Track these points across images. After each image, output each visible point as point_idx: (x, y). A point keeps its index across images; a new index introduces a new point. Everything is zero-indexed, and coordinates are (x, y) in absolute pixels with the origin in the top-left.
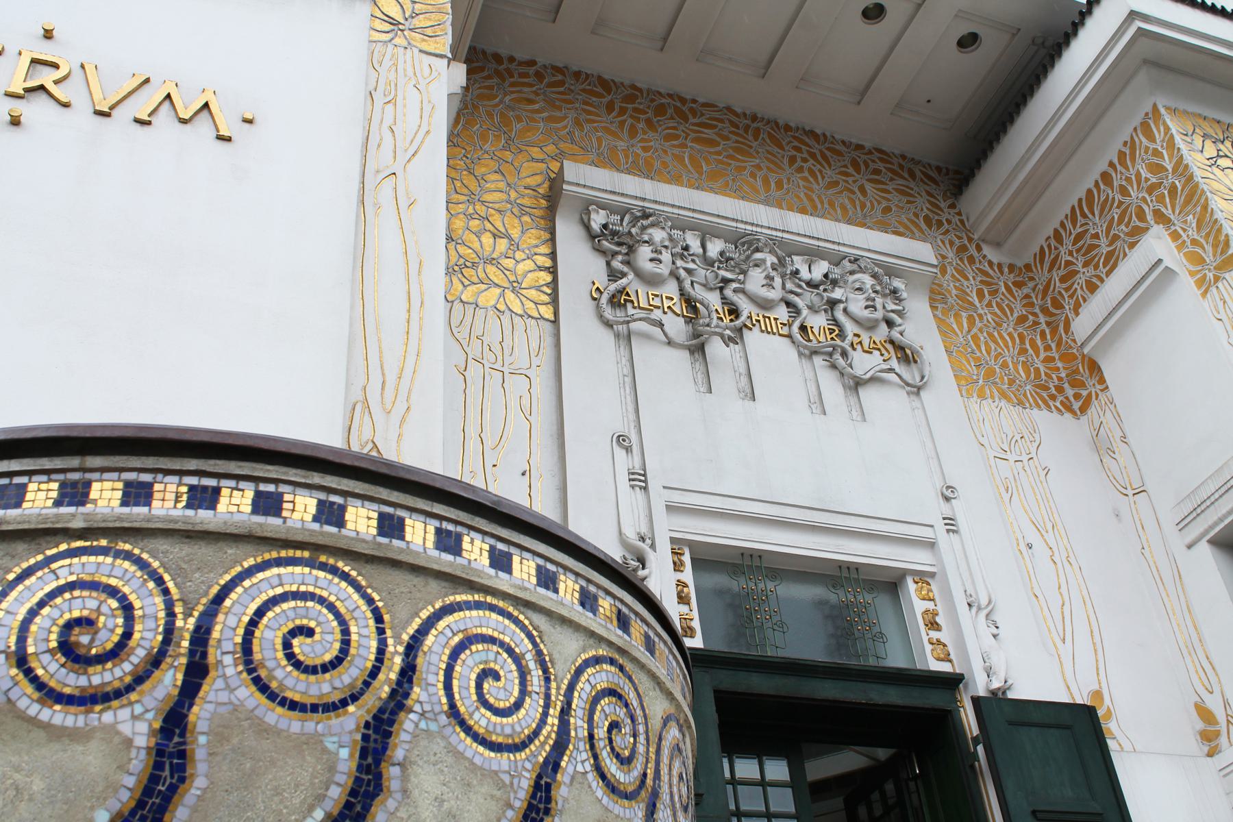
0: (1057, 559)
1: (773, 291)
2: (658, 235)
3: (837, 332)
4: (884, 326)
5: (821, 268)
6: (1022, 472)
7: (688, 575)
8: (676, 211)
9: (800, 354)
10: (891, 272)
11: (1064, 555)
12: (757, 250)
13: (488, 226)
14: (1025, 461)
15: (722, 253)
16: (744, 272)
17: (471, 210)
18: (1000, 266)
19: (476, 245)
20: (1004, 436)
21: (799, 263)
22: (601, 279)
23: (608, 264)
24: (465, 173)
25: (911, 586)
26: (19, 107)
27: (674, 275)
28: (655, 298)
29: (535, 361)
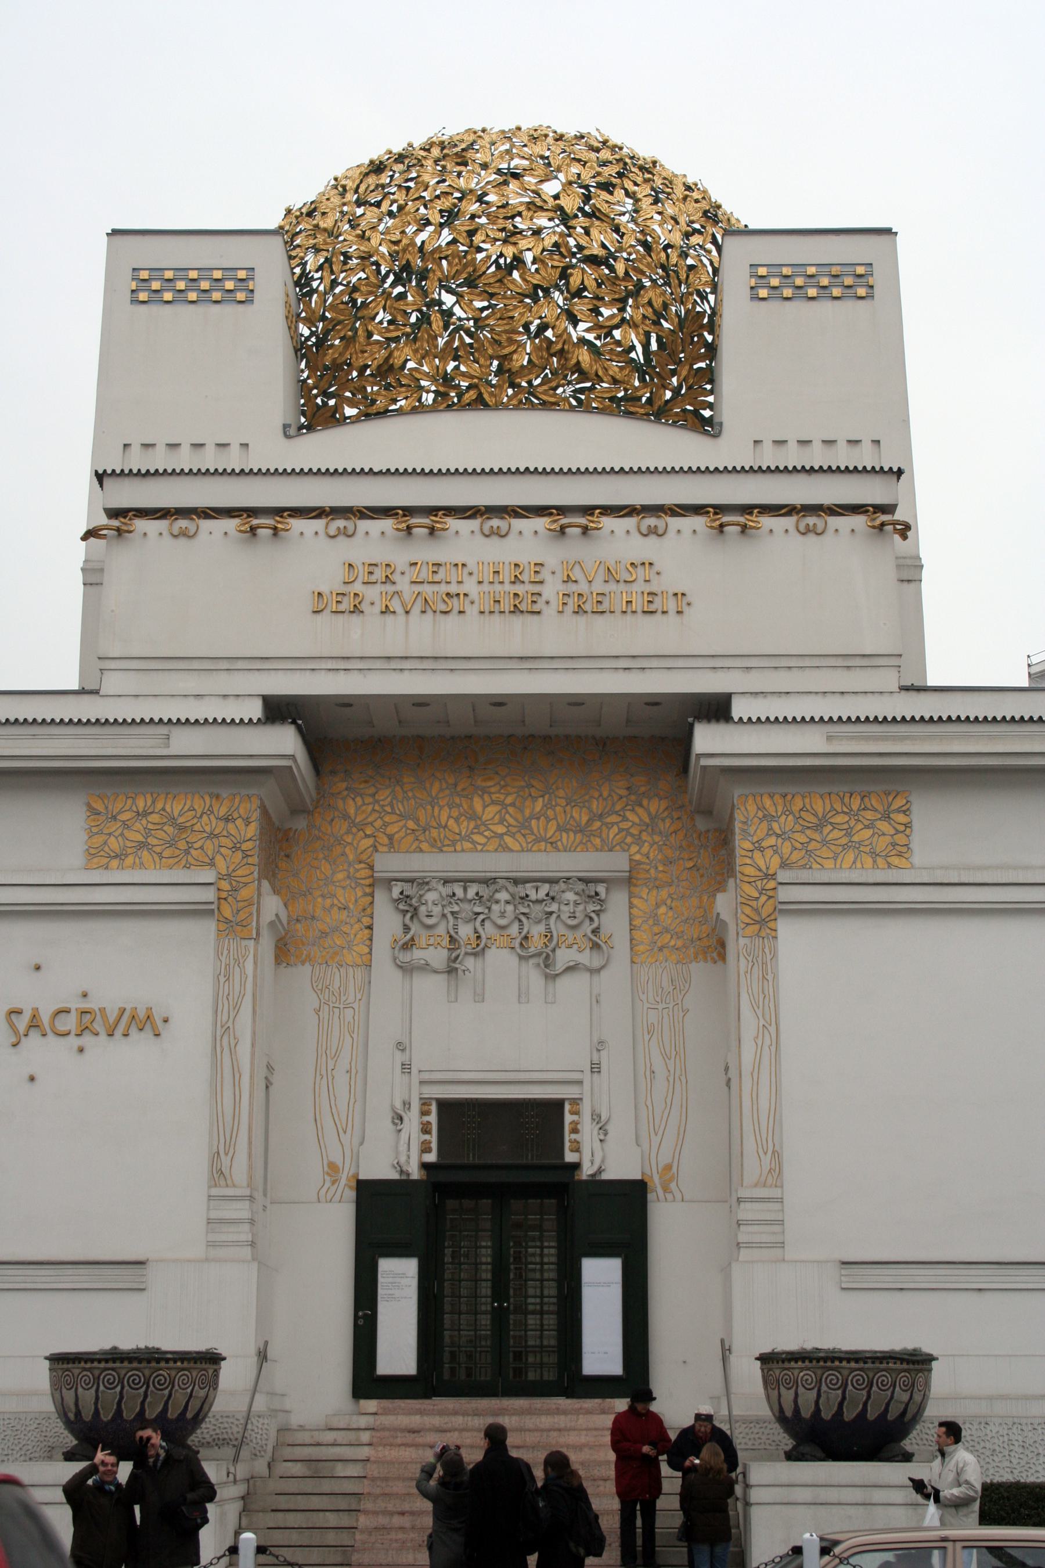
2: (431, 896)
3: (549, 934)
5: (545, 888)
6: (665, 1016)
7: (433, 1118)
9: (521, 957)
12: (496, 891)
14: (671, 1006)
15: (477, 894)
16: (489, 909)
17: (326, 891)
18: (708, 831)
19: (328, 920)
21: (529, 889)
22: (400, 930)
24: (324, 861)
27: (444, 916)
28: (432, 938)
29: (359, 997)
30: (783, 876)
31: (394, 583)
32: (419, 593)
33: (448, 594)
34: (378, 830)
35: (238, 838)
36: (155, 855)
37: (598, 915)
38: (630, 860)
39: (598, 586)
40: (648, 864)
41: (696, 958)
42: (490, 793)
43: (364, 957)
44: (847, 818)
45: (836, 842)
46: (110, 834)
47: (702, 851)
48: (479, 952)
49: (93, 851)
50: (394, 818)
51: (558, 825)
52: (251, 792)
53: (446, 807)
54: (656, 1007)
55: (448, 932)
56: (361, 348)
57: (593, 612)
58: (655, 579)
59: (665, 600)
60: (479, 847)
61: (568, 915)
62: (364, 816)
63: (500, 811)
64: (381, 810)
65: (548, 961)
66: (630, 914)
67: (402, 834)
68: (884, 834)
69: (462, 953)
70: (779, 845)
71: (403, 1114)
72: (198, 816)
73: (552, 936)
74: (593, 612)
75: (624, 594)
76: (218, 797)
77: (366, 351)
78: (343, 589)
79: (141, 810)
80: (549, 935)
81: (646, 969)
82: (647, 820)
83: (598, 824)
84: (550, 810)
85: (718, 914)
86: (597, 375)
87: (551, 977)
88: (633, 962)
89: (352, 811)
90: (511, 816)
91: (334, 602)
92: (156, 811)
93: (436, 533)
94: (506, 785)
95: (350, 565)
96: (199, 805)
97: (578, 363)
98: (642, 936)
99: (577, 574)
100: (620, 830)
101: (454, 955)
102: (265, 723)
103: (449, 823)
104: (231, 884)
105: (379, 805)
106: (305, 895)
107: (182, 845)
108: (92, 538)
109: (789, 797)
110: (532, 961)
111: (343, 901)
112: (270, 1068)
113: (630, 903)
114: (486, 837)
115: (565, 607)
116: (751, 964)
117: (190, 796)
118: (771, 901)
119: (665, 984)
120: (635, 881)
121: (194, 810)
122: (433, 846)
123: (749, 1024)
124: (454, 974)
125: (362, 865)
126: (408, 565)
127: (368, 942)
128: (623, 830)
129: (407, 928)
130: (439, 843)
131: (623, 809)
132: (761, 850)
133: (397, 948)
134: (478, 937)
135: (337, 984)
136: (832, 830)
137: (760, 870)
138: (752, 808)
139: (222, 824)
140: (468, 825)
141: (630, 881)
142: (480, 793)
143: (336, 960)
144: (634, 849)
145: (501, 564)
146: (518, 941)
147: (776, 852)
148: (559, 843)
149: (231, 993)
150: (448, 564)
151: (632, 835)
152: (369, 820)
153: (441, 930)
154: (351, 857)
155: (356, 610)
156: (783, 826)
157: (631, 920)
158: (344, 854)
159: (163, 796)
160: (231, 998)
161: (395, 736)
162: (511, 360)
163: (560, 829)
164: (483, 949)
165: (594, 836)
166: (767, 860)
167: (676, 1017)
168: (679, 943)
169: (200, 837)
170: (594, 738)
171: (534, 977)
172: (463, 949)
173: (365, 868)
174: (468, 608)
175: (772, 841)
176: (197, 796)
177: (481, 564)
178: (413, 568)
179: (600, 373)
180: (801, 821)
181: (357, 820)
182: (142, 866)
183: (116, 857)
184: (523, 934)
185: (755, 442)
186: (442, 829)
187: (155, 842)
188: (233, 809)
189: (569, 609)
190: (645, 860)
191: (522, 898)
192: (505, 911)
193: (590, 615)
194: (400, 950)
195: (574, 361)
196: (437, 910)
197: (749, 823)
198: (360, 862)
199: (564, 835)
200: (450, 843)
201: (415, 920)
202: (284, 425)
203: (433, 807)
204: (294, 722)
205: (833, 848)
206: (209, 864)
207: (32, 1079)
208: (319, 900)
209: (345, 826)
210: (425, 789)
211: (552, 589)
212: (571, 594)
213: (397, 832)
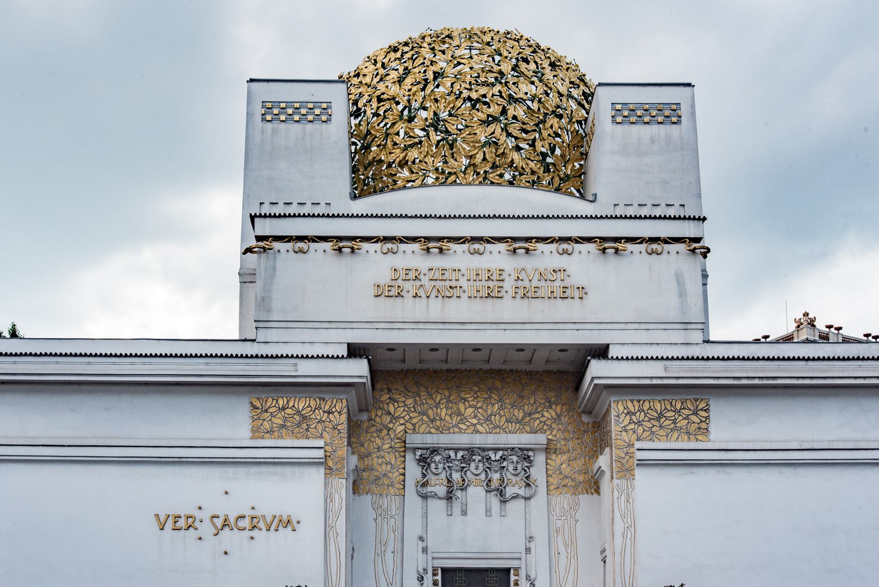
0: (569, 557)
1: (478, 470)
2: (437, 458)
4: (523, 471)
5: (500, 453)
7: (439, 578)
8: (445, 445)
10: (528, 450)
11: (573, 554)
12: (474, 455)
13: (384, 460)
15: (462, 456)
17: (379, 455)
19: (380, 470)
20: (563, 509)
21: (492, 454)
22: (420, 475)
23: (423, 468)
24: (377, 438)
25: (512, 572)
26: (252, 533)
27: (444, 468)
29: (398, 512)
30: (638, 445)
31: (420, 280)
32: (434, 286)
33: (451, 287)
34: (407, 421)
35: (336, 422)
36: (289, 432)
37: (529, 469)
38: (547, 439)
39: (535, 283)
40: (556, 441)
41: (583, 492)
42: (468, 401)
43: (400, 491)
44: (674, 414)
45: (668, 427)
46: (264, 420)
47: (585, 434)
48: (463, 489)
49: (255, 429)
50: (416, 414)
51: (506, 419)
52: (342, 397)
53: (444, 409)
54: (560, 518)
55: (447, 477)
56: (389, 151)
57: (532, 297)
58: (567, 278)
59: (572, 291)
60: (463, 431)
61: (513, 468)
62: (399, 413)
63: (474, 411)
64: (408, 410)
65: (501, 493)
66: (546, 468)
67: (420, 423)
68: (694, 423)
69: (455, 489)
70: (636, 428)
71: (423, 575)
72: (313, 410)
73: (504, 480)
74: (532, 297)
75: (550, 288)
76: (324, 399)
77: (393, 153)
78: (393, 283)
79: (281, 407)
80: (502, 480)
81: (555, 498)
82: (555, 417)
83: (527, 419)
84: (501, 411)
85: (600, 467)
86: (522, 168)
87: (504, 502)
88: (548, 494)
89: (392, 409)
90: (479, 413)
91: (387, 291)
92: (290, 407)
93: (618, 252)
94: (478, 397)
95: (395, 269)
96: (313, 403)
97: (512, 160)
98: (554, 480)
99: (523, 276)
100: (541, 422)
101: (450, 490)
102: (350, 358)
103: (446, 418)
104: (332, 448)
105: (407, 407)
106: (367, 457)
107: (304, 426)
108: (249, 253)
109: (642, 402)
110: (493, 493)
111: (388, 459)
112: (353, 550)
113: (546, 462)
114: (466, 425)
115: (516, 294)
116: (620, 494)
117: (308, 399)
118: (631, 460)
119: (566, 507)
120: (549, 450)
121: (311, 407)
122: (437, 430)
123: (619, 526)
124: (450, 500)
125: (398, 441)
126: (428, 270)
127: (403, 483)
128: (542, 422)
129: (424, 476)
130: (440, 428)
131: (542, 410)
132: (626, 431)
133: (419, 486)
134: (464, 480)
135: (385, 506)
136: (665, 420)
137: (626, 442)
138: (621, 408)
139: (326, 415)
140: (457, 419)
141: (549, 449)
142: (463, 401)
143: (385, 492)
144: (548, 432)
145: (480, 270)
146: (486, 482)
147: (634, 432)
148: (507, 429)
149: (334, 508)
150: (450, 269)
151: (547, 425)
152: (402, 415)
153: (443, 476)
154: (392, 436)
155: (399, 295)
156: (638, 418)
157: (547, 471)
158: (388, 434)
159: (293, 399)
160: (333, 510)
161: (415, 369)
162: (475, 158)
163: (507, 421)
164: (466, 486)
165: (526, 425)
166: (630, 438)
167: (571, 524)
168: (573, 484)
169: (314, 422)
170: (525, 371)
171: (495, 502)
172: (455, 486)
173: (400, 442)
174: (462, 294)
175: (632, 426)
176: (312, 399)
177: (469, 270)
178: (431, 271)
179: (524, 166)
180: (647, 415)
181: (396, 415)
182: (280, 437)
183: (268, 432)
184: (488, 478)
185: (614, 205)
186: (442, 421)
187: (289, 424)
188: (332, 407)
189: (518, 296)
190: (554, 438)
191: (487, 459)
192: (478, 466)
193: (530, 299)
194: (420, 487)
195: (510, 159)
196: (441, 466)
197: (620, 416)
198: (398, 439)
199: (510, 424)
200: (447, 428)
201: (428, 471)
202: (350, 193)
203: (437, 409)
204: (367, 357)
205: (666, 430)
206: (320, 437)
207: (226, 553)
208: (376, 459)
209: (389, 419)
210: (432, 398)
211: (509, 284)
212: (520, 287)
213: (417, 423)
